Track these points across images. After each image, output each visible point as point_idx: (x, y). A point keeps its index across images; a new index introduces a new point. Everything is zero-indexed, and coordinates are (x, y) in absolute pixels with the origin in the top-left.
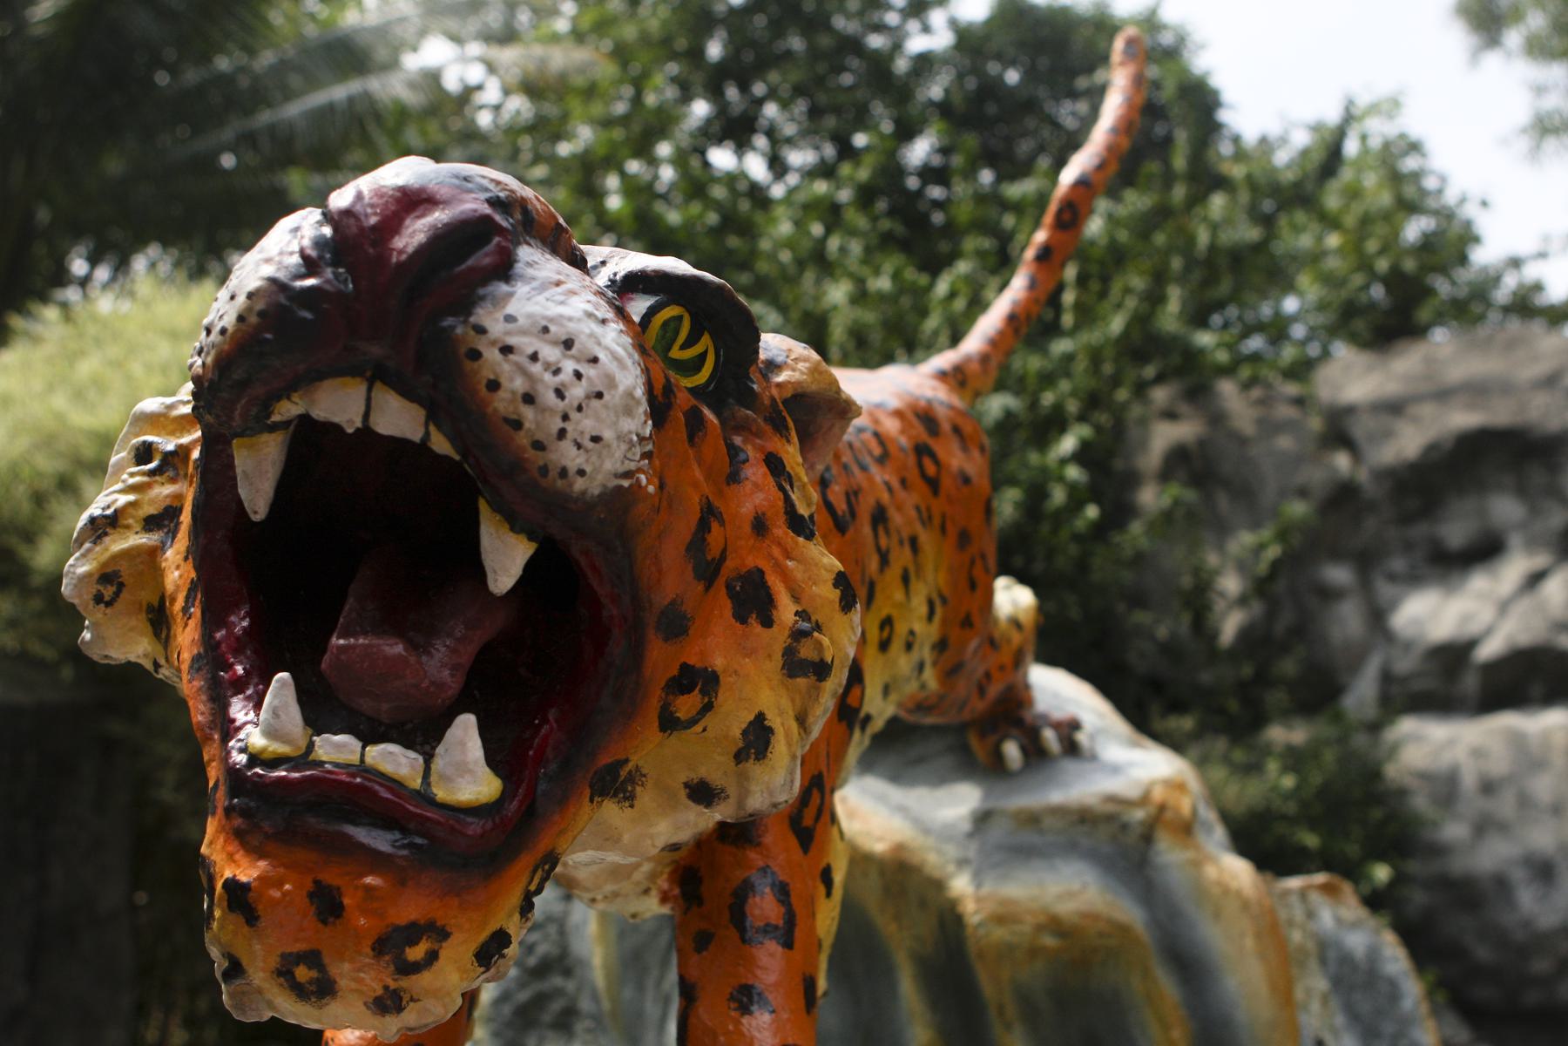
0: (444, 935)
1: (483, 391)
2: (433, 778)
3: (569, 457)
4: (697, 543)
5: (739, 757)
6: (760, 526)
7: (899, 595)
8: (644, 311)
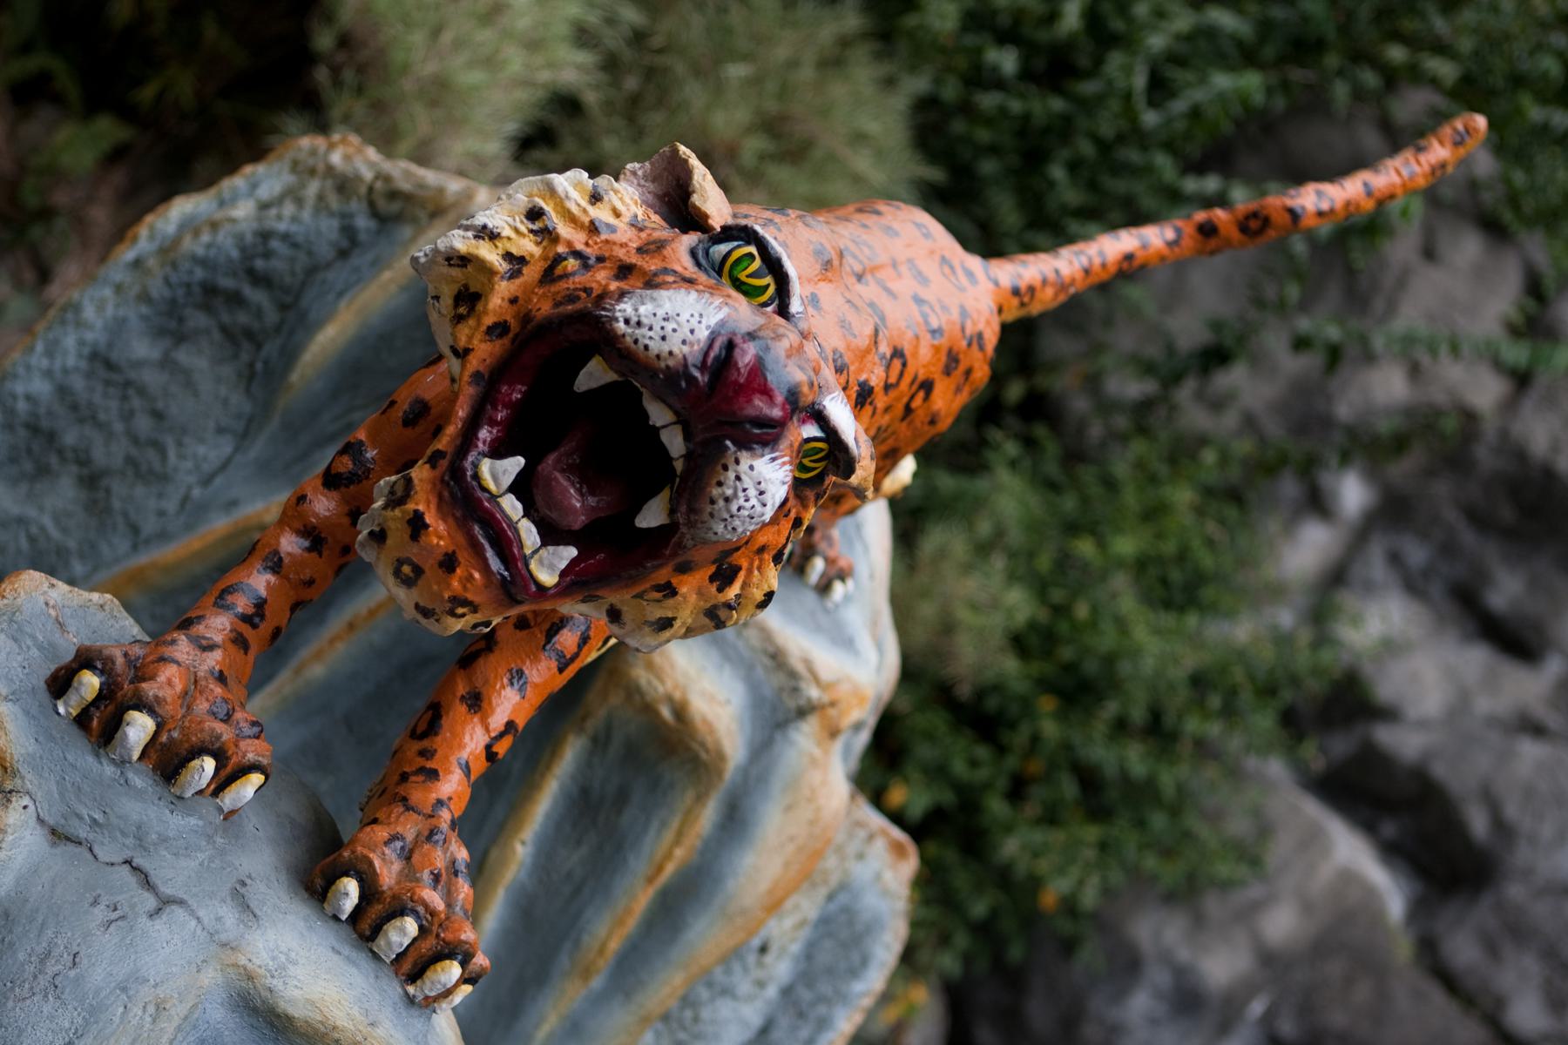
1: (714, 481)
2: (536, 557)
8: (812, 436)
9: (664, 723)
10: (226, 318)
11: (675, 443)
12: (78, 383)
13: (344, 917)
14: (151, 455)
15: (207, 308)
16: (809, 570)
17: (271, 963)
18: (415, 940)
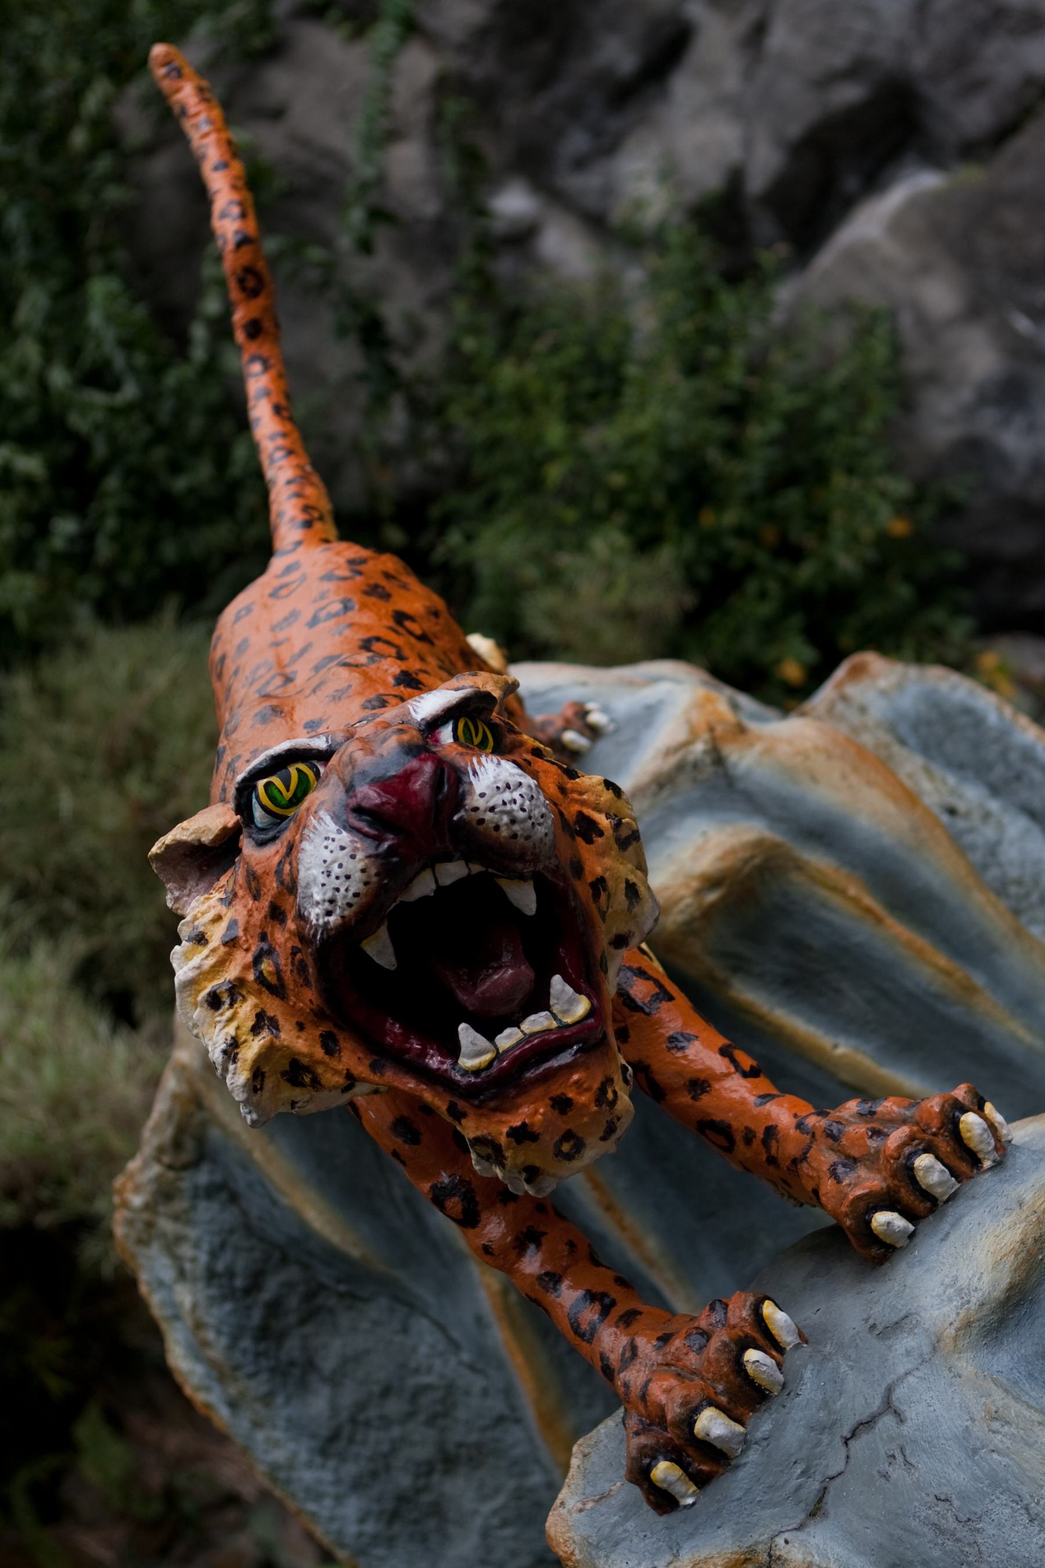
1: (494, 833)
2: (560, 1016)
8: (452, 734)
9: (722, 899)
10: (292, 1319)
11: (453, 871)
12: (350, 1470)
13: (911, 1228)
14: (425, 1400)
15: (281, 1337)
16: (574, 747)
17: (955, 1303)
18: (938, 1158)
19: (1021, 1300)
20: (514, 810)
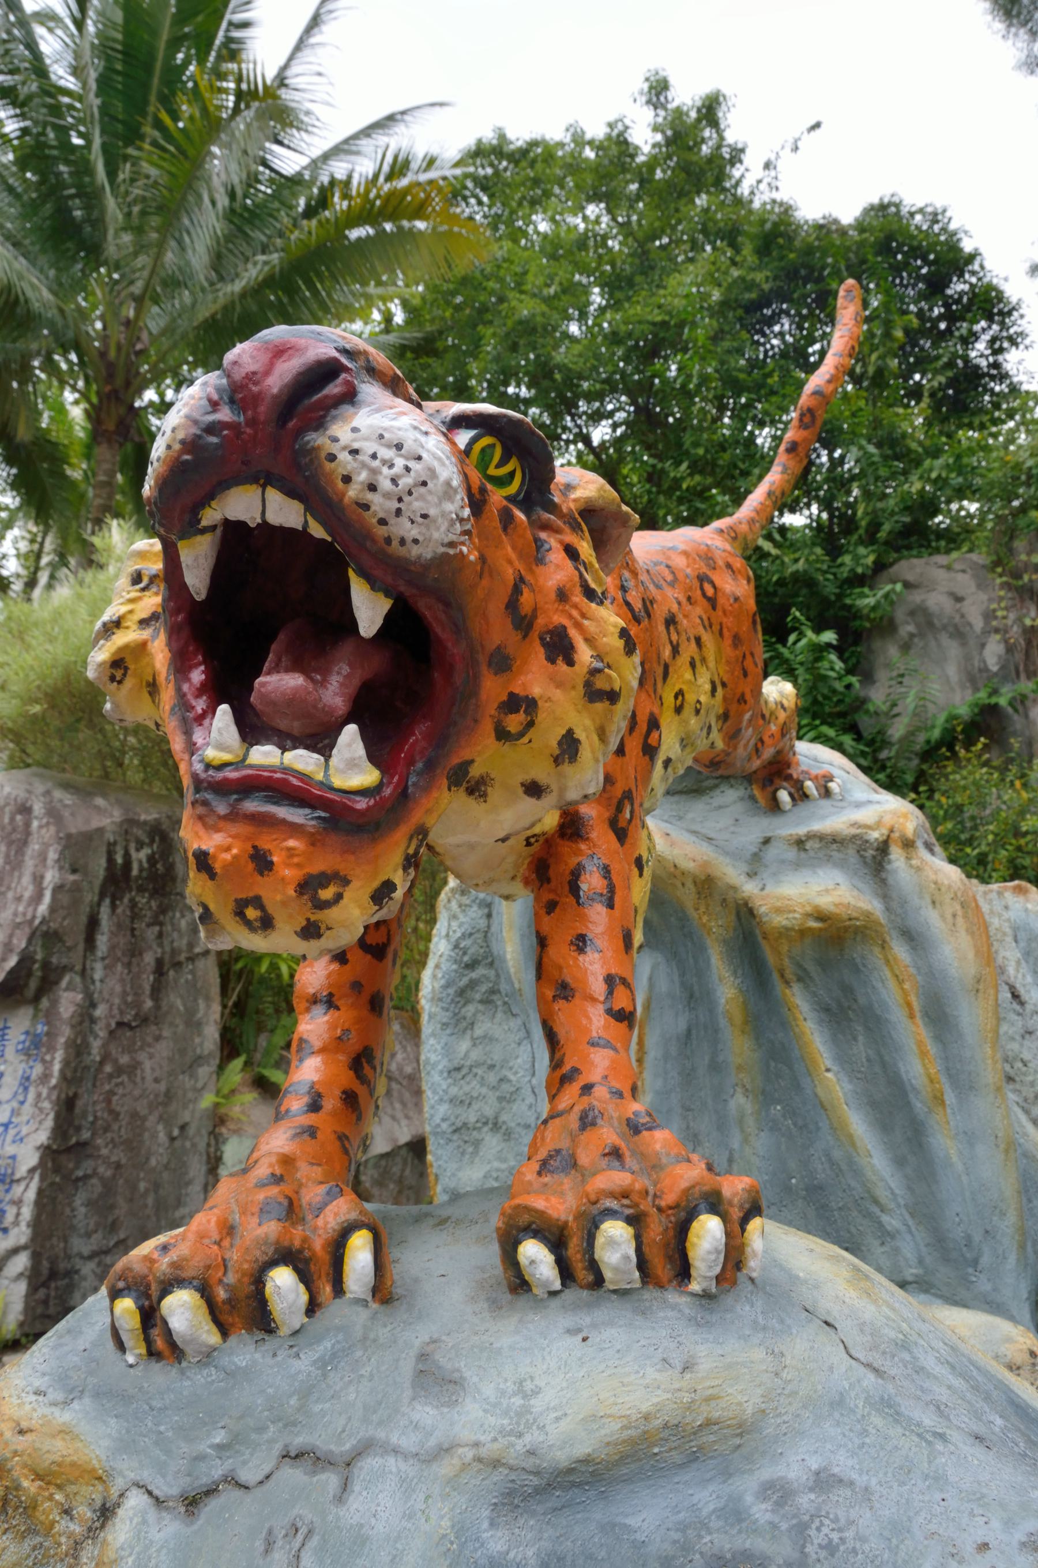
0: (346, 882)
1: (340, 485)
2: (331, 771)
3: (404, 528)
4: (512, 605)
5: (557, 761)
6: (562, 595)
7: (688, 675)
9: (820, 929)
10: (478, 996)
12: (454, 1091)
13: (557, 1285)
14: (505, 1087)
15: (467, 1002)
16: (808, 792)
17: (506, 1422)
18: (638, 1238)
19: (587, 1483)
20: (381, 473)
